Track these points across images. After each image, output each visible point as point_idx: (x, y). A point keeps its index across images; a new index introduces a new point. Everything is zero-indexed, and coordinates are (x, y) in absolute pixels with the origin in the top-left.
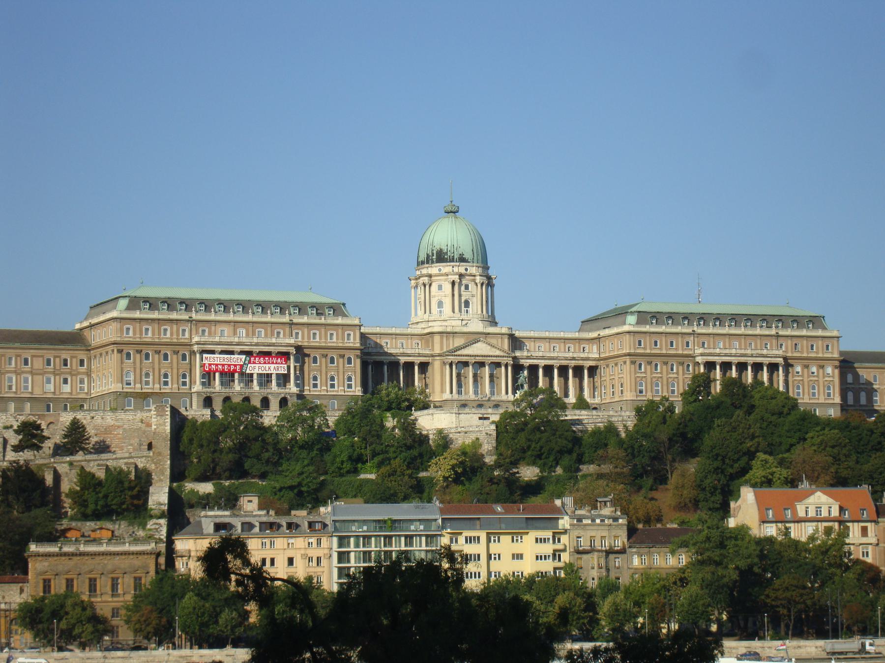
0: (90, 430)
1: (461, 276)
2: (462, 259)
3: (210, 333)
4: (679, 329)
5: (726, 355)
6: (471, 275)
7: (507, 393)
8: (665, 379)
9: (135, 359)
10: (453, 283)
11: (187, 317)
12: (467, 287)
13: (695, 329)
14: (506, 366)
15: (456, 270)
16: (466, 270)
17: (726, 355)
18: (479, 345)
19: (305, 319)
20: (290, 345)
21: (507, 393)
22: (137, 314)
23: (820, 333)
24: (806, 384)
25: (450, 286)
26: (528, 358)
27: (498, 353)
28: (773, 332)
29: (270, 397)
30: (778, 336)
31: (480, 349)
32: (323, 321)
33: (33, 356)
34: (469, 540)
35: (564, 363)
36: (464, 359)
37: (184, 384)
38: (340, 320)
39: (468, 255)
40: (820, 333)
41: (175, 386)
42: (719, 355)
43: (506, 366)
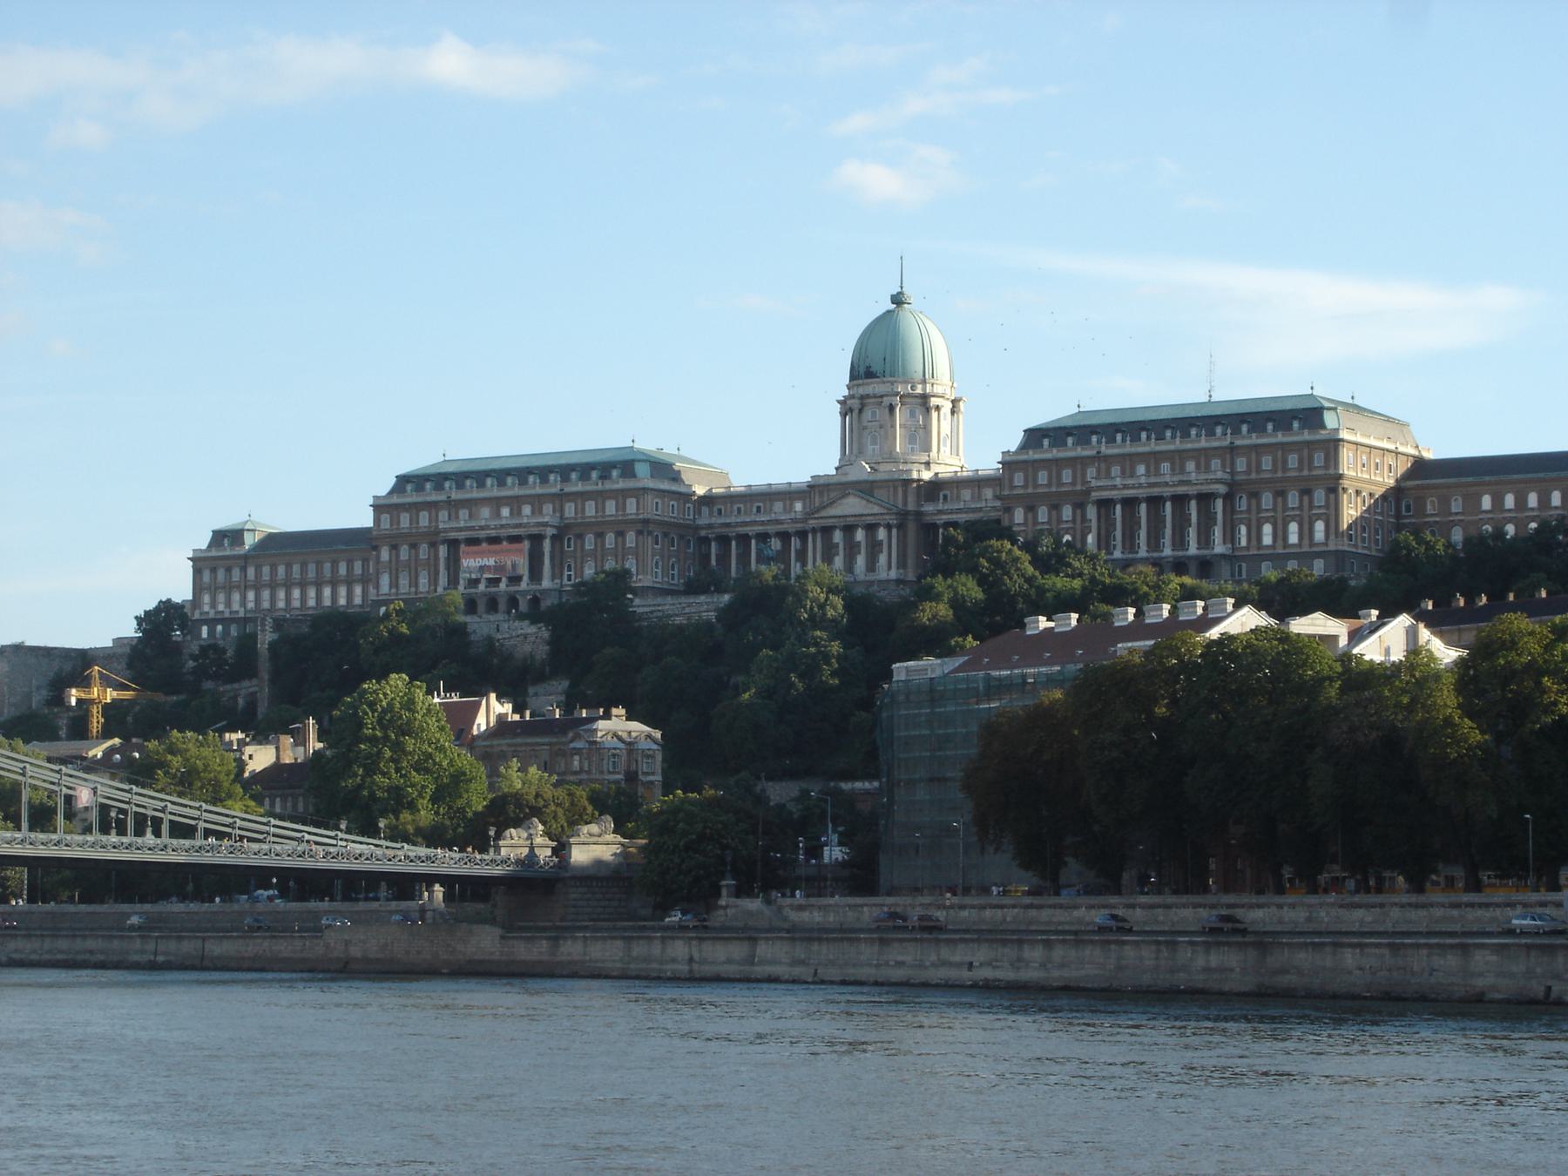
1: (862, 398)
2: (870, 374)
3: (471, 516)
4: (1080, 452)
5: (1125, 487)
7: (890, 568)
11: (443, 497)
12: (874, 414)
13: (1103, 449)
15: (861, 391)
17: (1125, 487)
19: (580, 487)
20: (545, 525)
21: (890, 568)
22: (395, 500)
23: (1307, 436)
24: (1280, 522)
27: (876, 510)
28: (1227, 443)
30: (1232, 449)
31: (852, 506)
32: (600, 487)
36: (830, 522)
38: (621, 485)
39: (876, 368)
40: (1307, 436)
42: (1114, 487)
43: (889, 527)
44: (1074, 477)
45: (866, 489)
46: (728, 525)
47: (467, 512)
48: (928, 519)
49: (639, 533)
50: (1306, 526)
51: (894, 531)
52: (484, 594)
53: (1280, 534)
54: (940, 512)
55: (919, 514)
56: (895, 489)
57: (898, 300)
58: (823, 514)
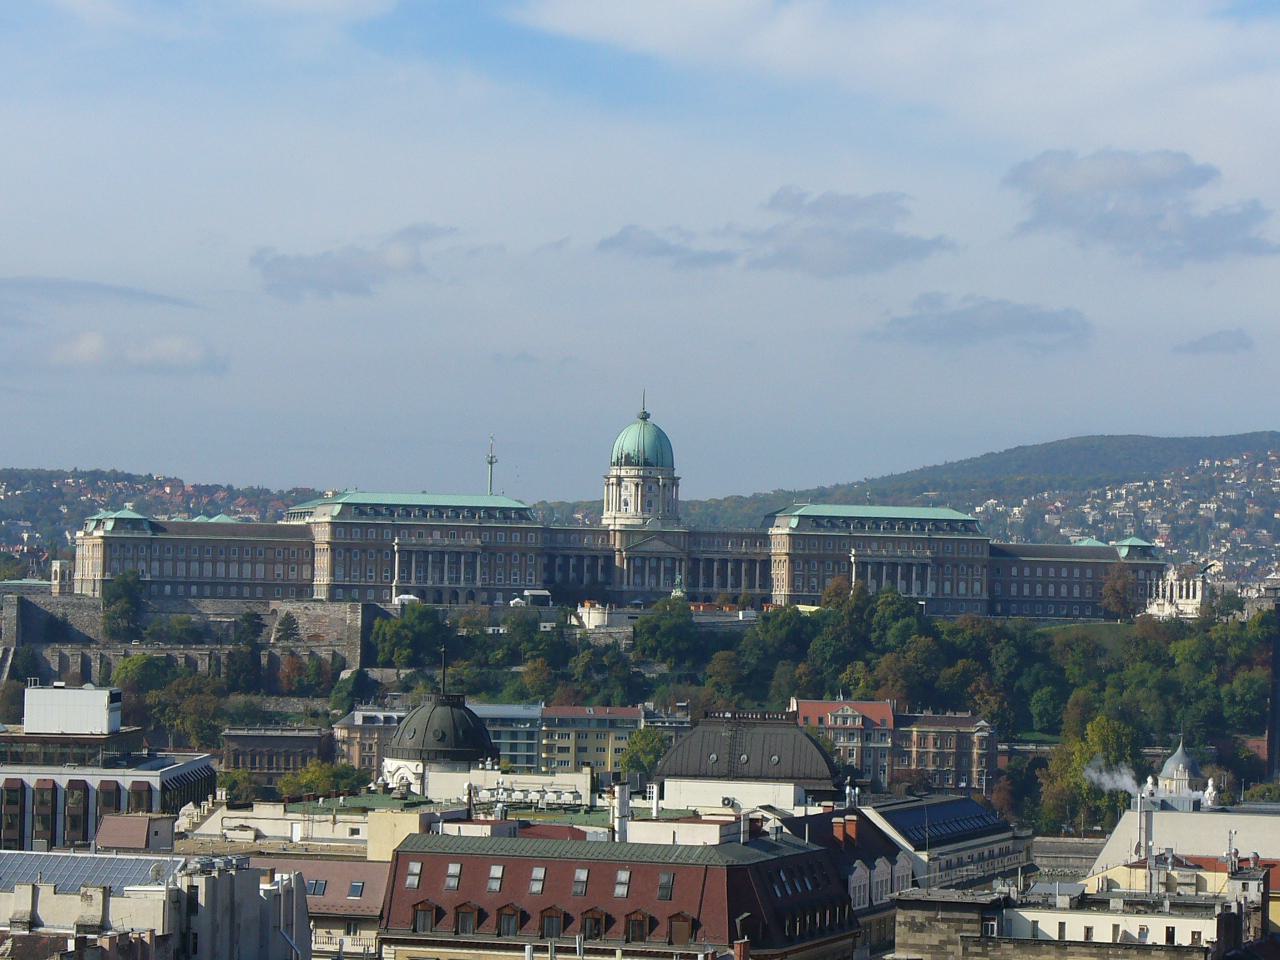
0: (302, 621)
6: (653, 478)
8: (821, 578)
9: (345, 556)
10: (637, 485)
12: (650, 488)
14: (681, 560)
15: (641, 473)
16: (650, 473)
17: (877, 556)
18: (656, 542)
20: (478, 546)
24: (955, 581)
25: (633, 488)
26: (703, 552)
27: (672, 549)
29: (458, 591)
31: (657, 546)
33: (266, 549)
34: (561, 736)
35: (739, 557)
37: (387, 577)
41: (379, 579)
44: (834, 546)
45: (662, 535)
46: (555, 548)
47: (406, 532)
48: (694, 556)
49: (537, 555)
50: (970, 586)
51: (683, 564)
52: (432, 588)
53: (955, 587)
54: (703, 552)
55: (693, 552)
56: (679, 537)
57: (645, 417)
58: (636, 549)
